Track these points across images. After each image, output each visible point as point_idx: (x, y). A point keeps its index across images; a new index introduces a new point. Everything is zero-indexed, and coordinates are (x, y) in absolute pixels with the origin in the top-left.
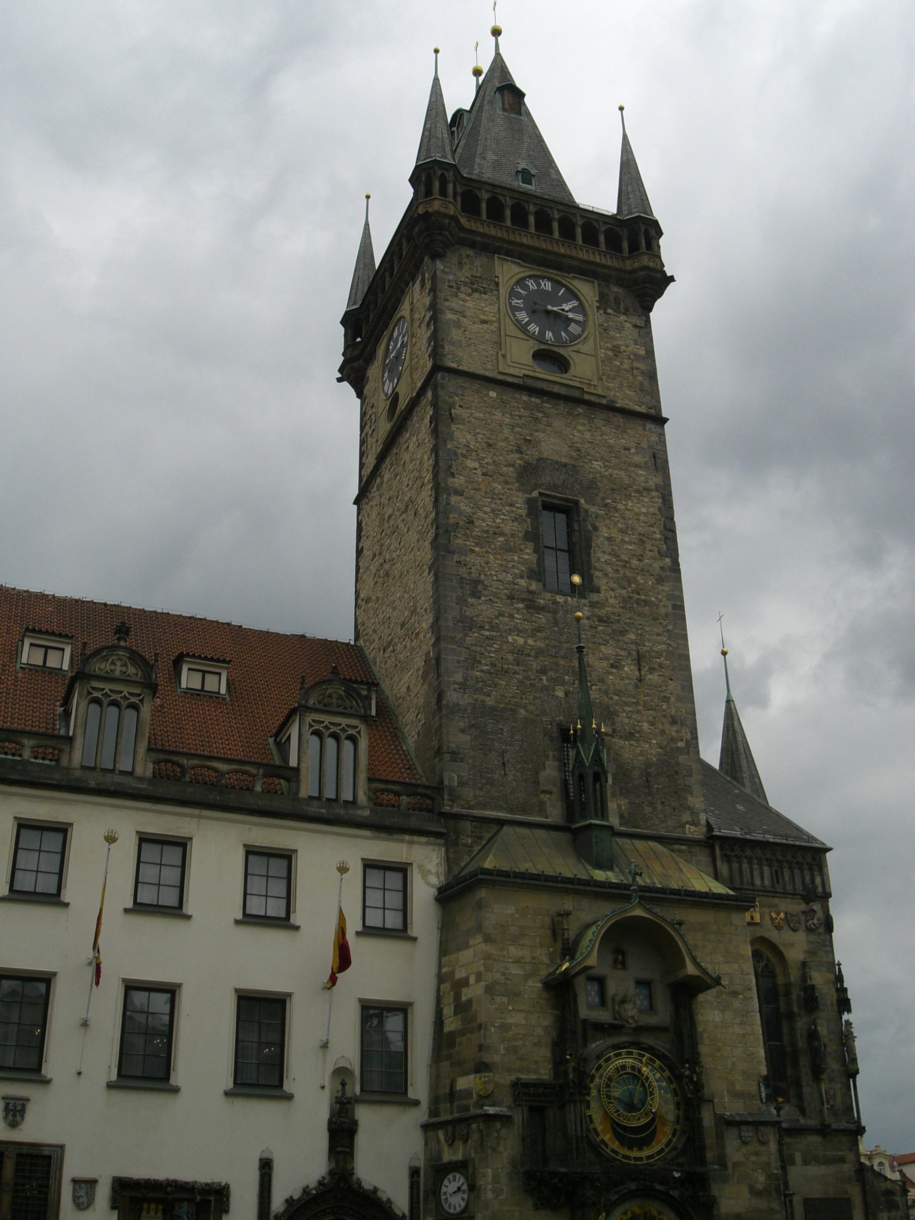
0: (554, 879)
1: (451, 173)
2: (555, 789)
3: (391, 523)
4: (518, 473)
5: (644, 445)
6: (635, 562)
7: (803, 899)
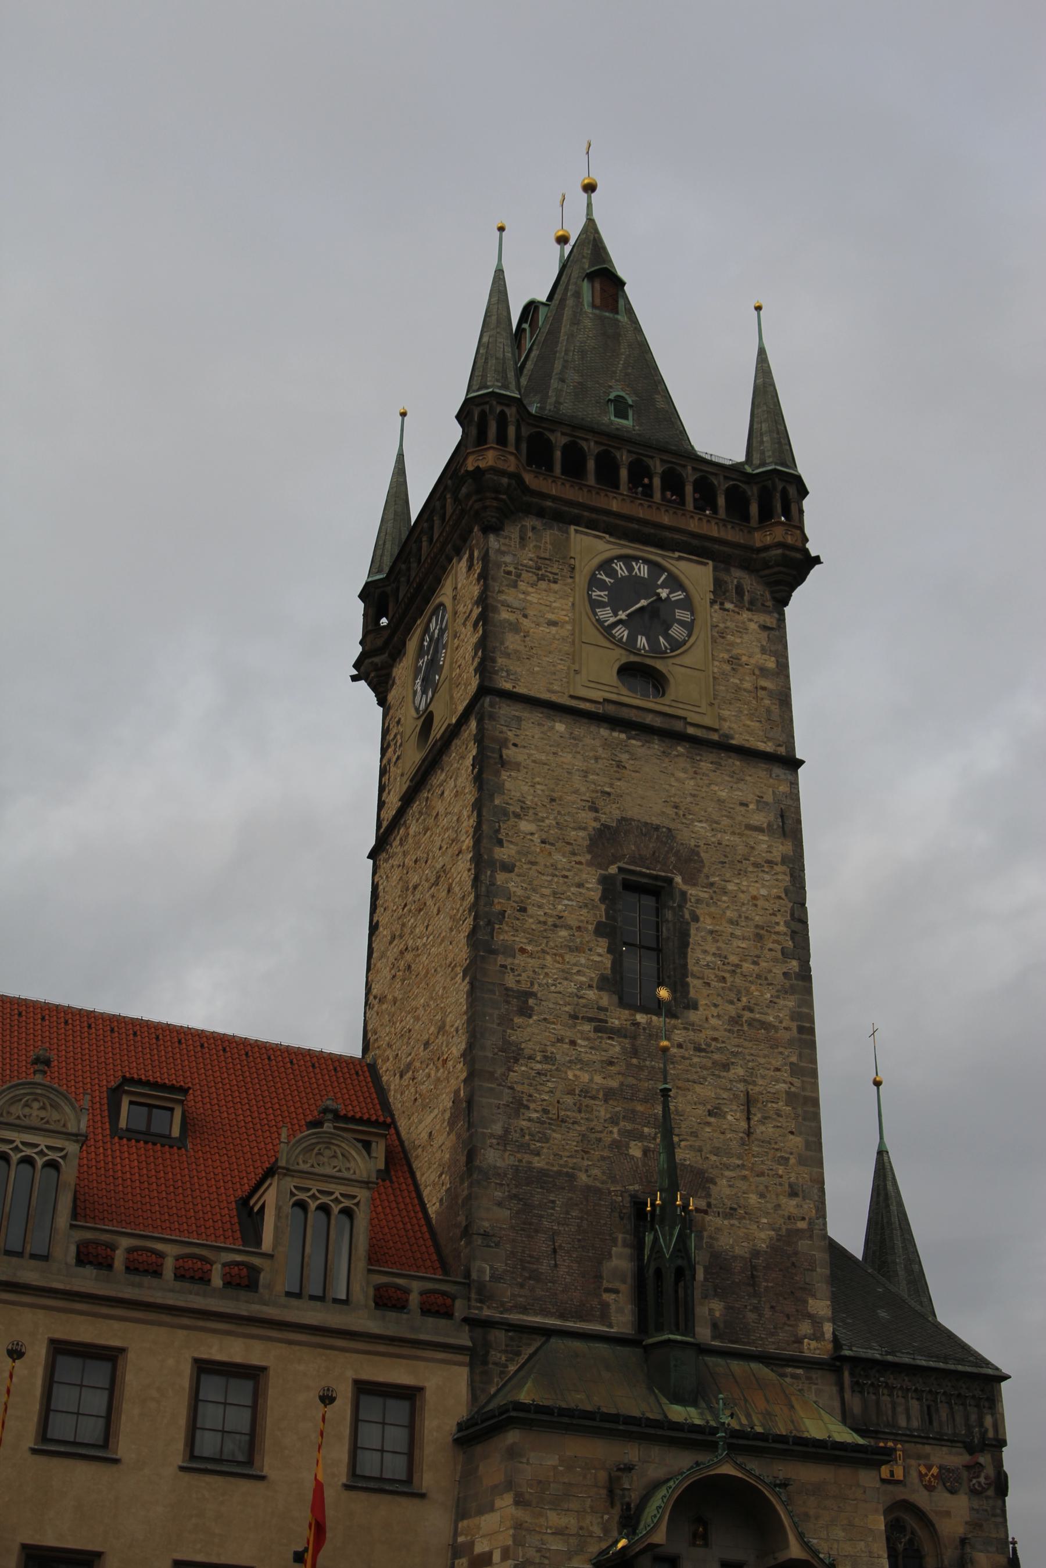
0: (615, 1418)
1: (514, 410)
2: (625, 1288)
3: (417, 897)
4: (591, 840)
5: (769, 798)
6: (747, 966)
7: (965, 1447)
